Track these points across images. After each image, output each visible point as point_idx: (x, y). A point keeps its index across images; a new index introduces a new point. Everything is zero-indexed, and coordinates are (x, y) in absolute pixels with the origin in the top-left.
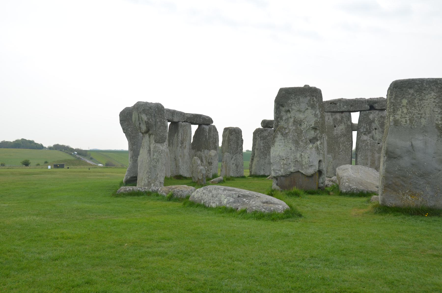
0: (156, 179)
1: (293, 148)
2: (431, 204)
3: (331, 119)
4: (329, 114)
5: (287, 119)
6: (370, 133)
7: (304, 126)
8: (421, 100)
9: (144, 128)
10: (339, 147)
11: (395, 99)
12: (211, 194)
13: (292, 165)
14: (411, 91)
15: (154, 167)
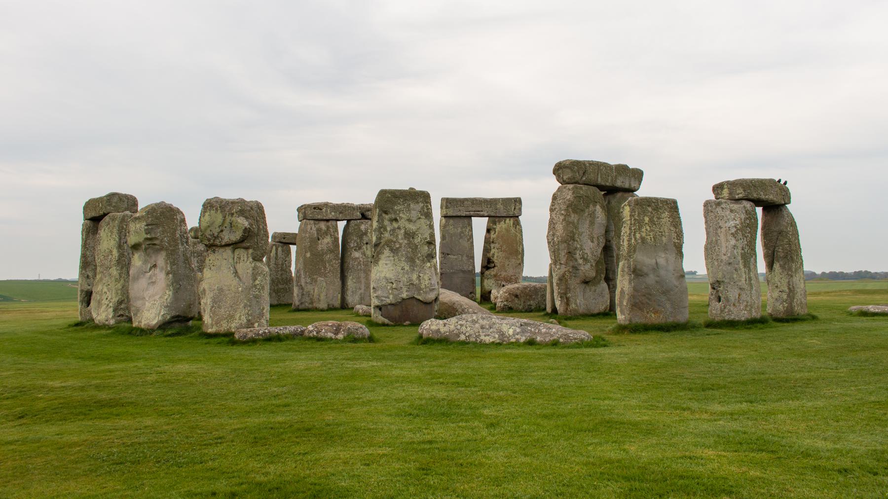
0: (262, 315)
1: (407, 268)
2: (671, 320)
3: (314, 229)
4: (312, 222)
5: (394, 230)
6: (360, 248)
7: (417, 241)
8: (659, 218)
9: (236, 236)
10: (325, 268)
11: (639, 216)
12: (477, 325)
13: (405, 289)
14: (650, 209)
15: (256, 297)
